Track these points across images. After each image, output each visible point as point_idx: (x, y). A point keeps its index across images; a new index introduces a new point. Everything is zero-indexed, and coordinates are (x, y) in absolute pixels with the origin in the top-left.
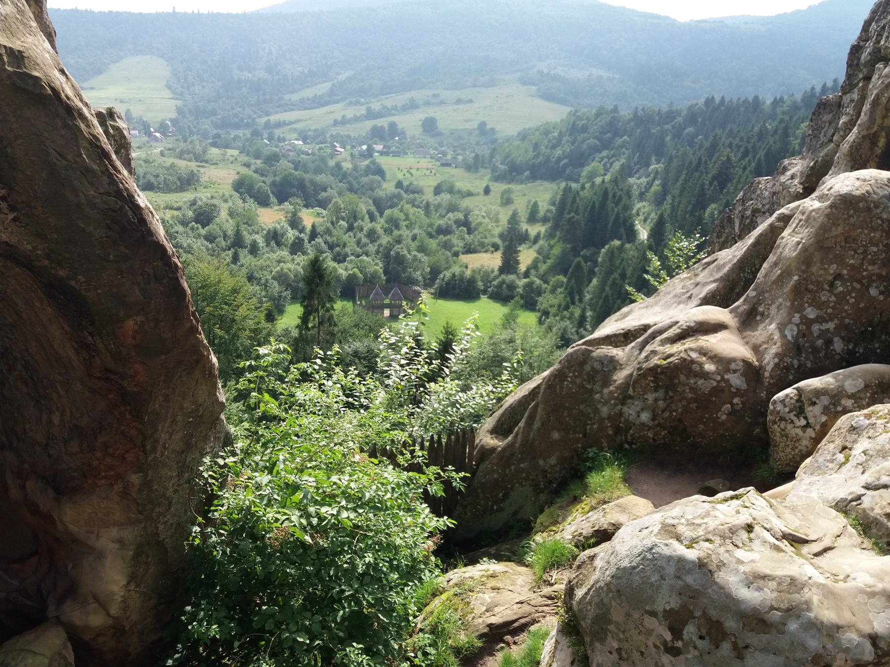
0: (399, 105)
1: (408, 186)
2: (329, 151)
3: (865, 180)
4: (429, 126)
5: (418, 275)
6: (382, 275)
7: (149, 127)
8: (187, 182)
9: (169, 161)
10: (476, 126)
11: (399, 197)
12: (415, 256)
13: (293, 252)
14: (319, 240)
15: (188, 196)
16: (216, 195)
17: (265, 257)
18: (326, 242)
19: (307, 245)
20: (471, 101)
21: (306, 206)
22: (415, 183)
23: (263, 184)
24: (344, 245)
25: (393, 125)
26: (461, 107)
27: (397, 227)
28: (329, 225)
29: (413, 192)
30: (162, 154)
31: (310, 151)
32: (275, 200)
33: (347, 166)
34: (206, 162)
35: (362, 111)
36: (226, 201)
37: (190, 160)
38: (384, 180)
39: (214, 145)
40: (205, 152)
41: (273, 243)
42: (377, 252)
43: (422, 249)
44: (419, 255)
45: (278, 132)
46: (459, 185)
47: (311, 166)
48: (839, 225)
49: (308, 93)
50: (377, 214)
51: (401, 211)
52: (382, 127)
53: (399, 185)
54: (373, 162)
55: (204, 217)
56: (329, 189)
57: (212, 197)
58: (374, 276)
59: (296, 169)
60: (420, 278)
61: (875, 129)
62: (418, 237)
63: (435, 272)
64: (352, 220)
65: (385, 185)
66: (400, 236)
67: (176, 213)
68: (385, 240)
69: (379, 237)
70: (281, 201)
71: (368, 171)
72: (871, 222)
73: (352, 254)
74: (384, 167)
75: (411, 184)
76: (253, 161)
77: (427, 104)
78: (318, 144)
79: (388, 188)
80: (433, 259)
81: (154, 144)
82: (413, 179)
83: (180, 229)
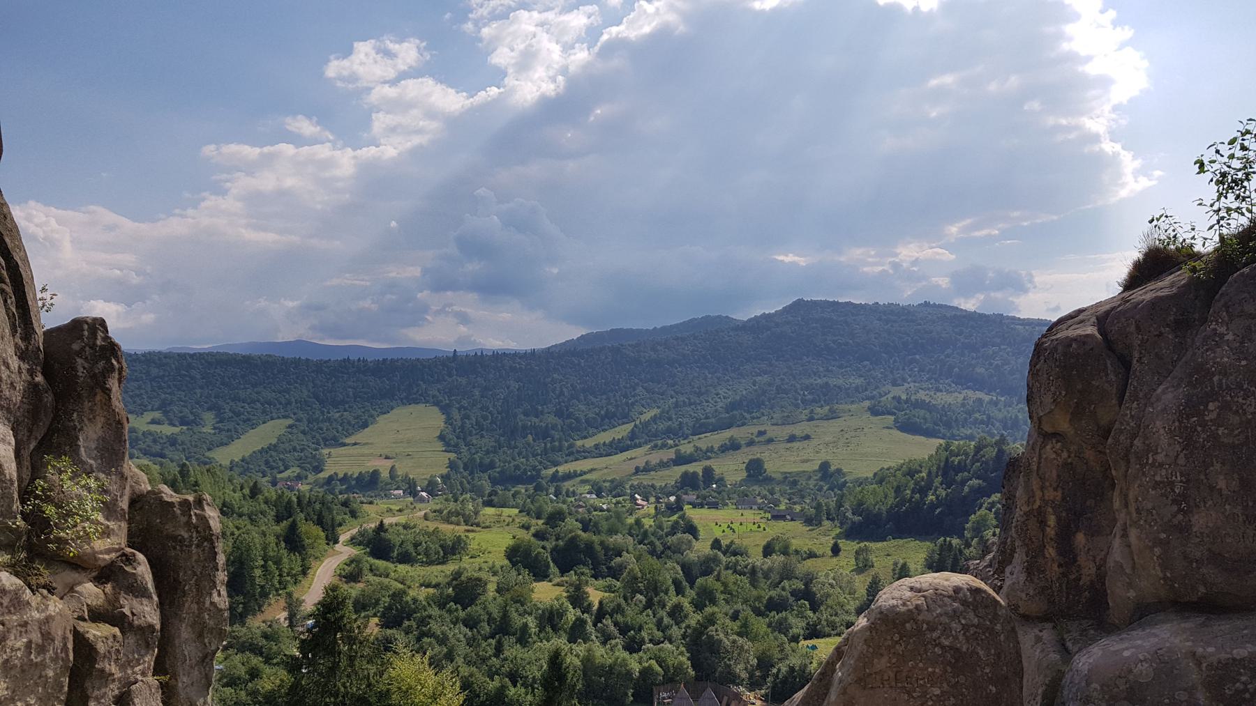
0: (716, 446)
1: (728, 547)
2: (628, 505)
3: (919, 591)
4: (755, 470)
5: (739, 669)
6: (690, 670)
7: (415, 486)
8: (453, 549)
9: (431, 526)
10: (817, 467)
11: (715, 560)
12: (734, 642)
13: (572, 640)
14: (608, 621)
15: (450, 568)
16: (485, 566)
17: (536, 646)
18: (616, 624)
19: (590, 628)
20: (807, 437)
21: (595, 577)
22: (737, 541)
23: (544, 550)
24: (640, 628)
25: (708, 472)
26: (796, 445)
27: (713, 601)
28: (622, 601)
29: (735, 554)
30: (426, 517)
31: (605, 507)
32: (556, 570)
33: (648, 523)
34: (478, 525)
35: (671, 454)
36: (495, 574)
37: (458, 524)
38: (697, 539)
39: (489, 504)
40: (476, 513)
41: (548, 629)
42: (684, 637)
43: (744, 632)
44: (740, 641)
45: (567, 485)
46: (795, 544)
47: (604, 525)
48: (882, 655)
49: (605, 437)
50: (685, 583)
51: (718, 579)
52: (695, 474)
53: (716, 544)
54: (682, 517)
55: (464, 592)
56: (624, 553)
57: (480, 569)
58: (679, 669)
59: (585, 530)
60: (744, 675)
61: (1038, 503)
62: (741, 616)
63: (765, 663)
64: (651, 594)
65: (697, 545)
66: (713, 614)
67: (431, 590)
68: (694, 619)
69: (686, 616)
70: (563, 571)
71: (674, 529)
72: (926, 651)
73: (651, 641)
74: (696, 522)
75: (732, 542)
76: (534, 521)
77: (751, 443)
78: (615, 497)
79: (701, 548)
80: (760, 646)
81: (419, 506)
82: (736, 536)
83: (435, 611)
